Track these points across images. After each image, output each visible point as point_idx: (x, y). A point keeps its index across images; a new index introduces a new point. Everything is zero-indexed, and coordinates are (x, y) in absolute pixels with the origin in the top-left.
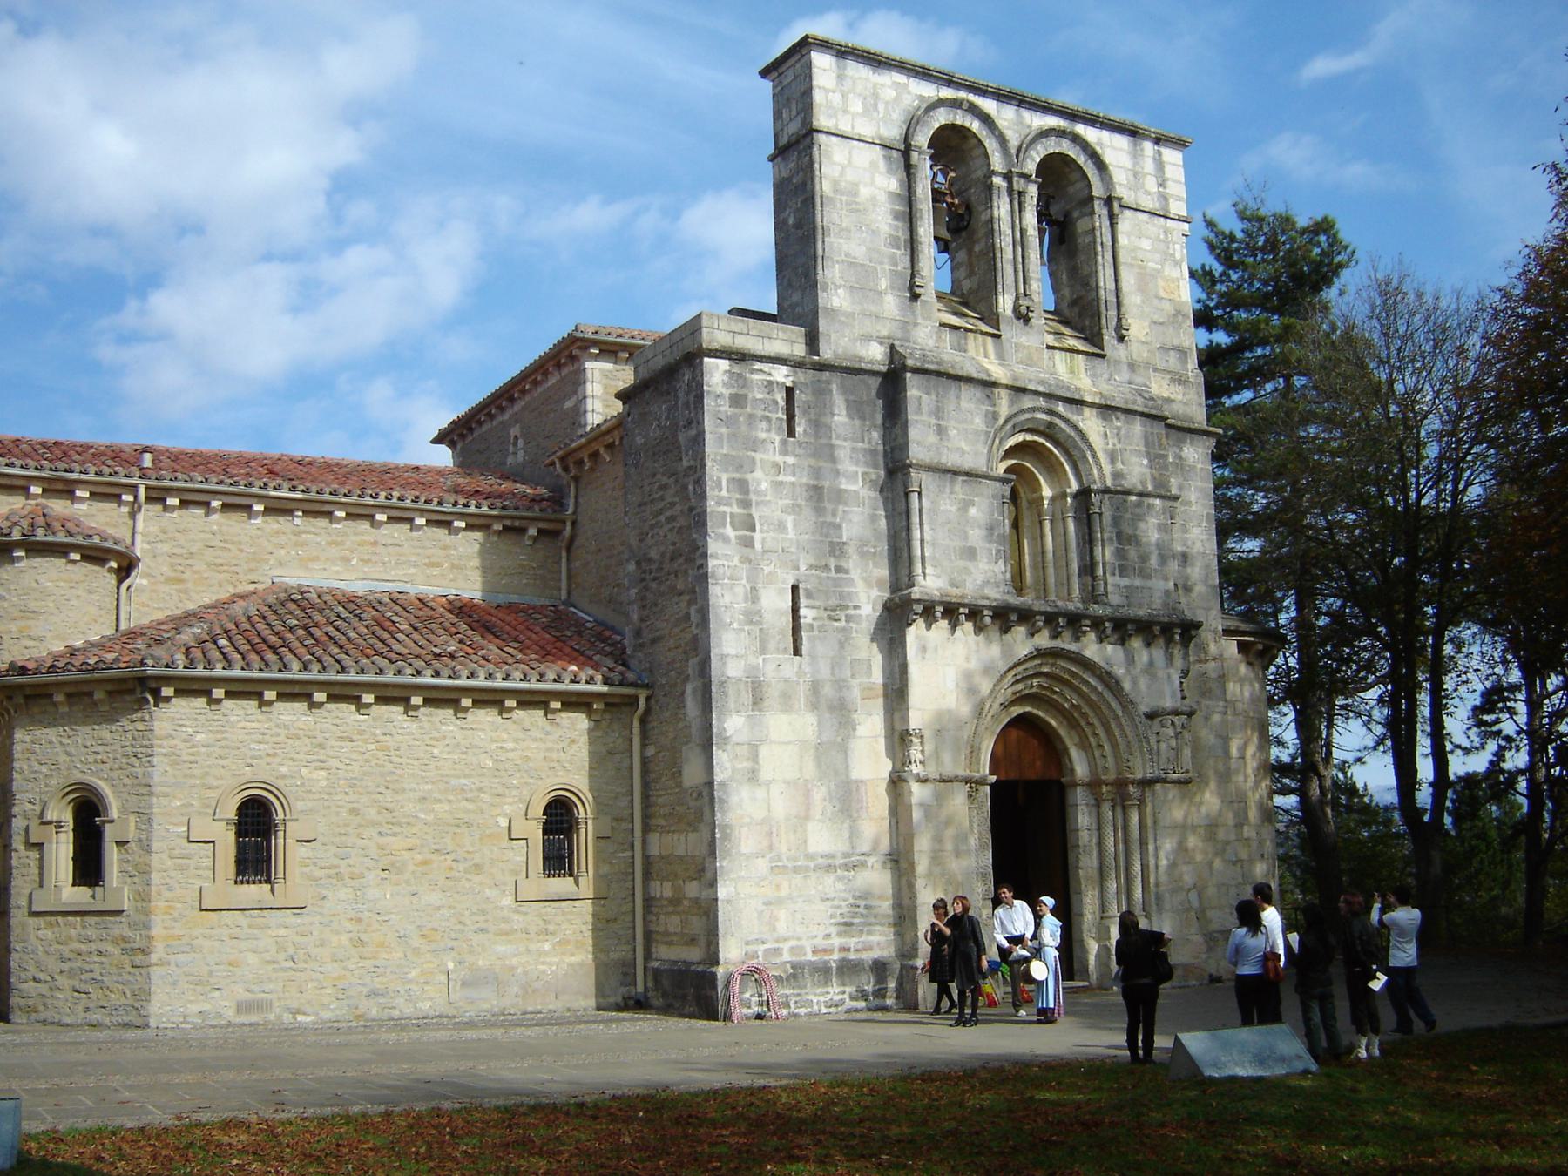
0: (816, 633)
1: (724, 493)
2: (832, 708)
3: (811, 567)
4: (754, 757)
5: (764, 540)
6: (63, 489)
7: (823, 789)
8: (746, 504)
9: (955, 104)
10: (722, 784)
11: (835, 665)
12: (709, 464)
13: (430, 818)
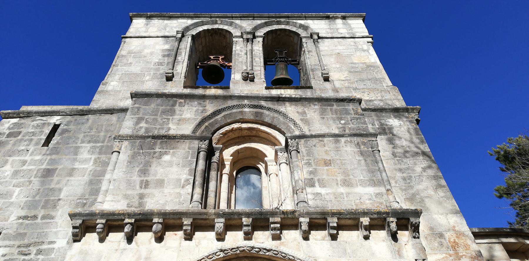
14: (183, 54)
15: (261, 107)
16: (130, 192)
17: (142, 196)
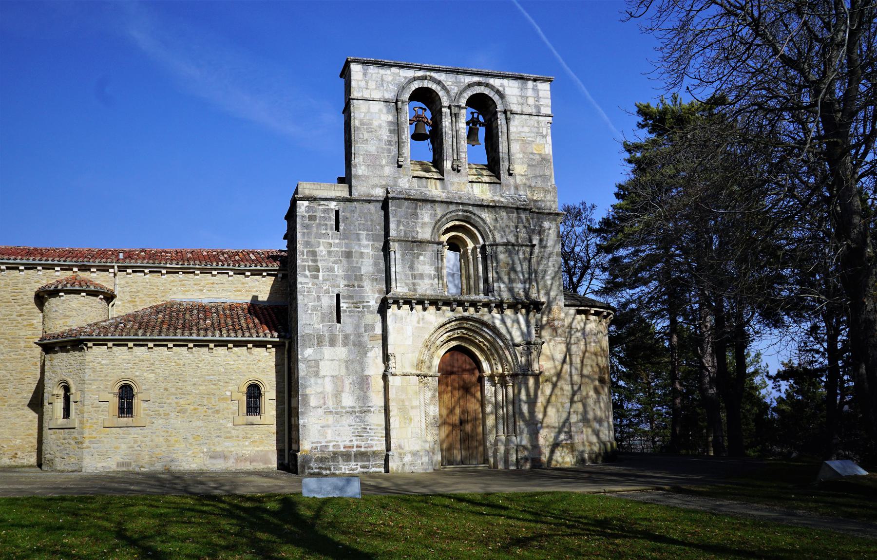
0: (348, 313)
1: (305, 257)
2: (355, 345)
3: (346, 286)
4: (318, 367)
5: (323, 275)
6: (85, 268)
7: (351, 379)
8: (315, 261)
9: (424, 78)
10: (304, 378)
11: (357, 326)
12: (298, 245)
13: (197, 392)
14: (406, 130)
15: (470, 212)
16: (407, 281)
17: (414, 284)
